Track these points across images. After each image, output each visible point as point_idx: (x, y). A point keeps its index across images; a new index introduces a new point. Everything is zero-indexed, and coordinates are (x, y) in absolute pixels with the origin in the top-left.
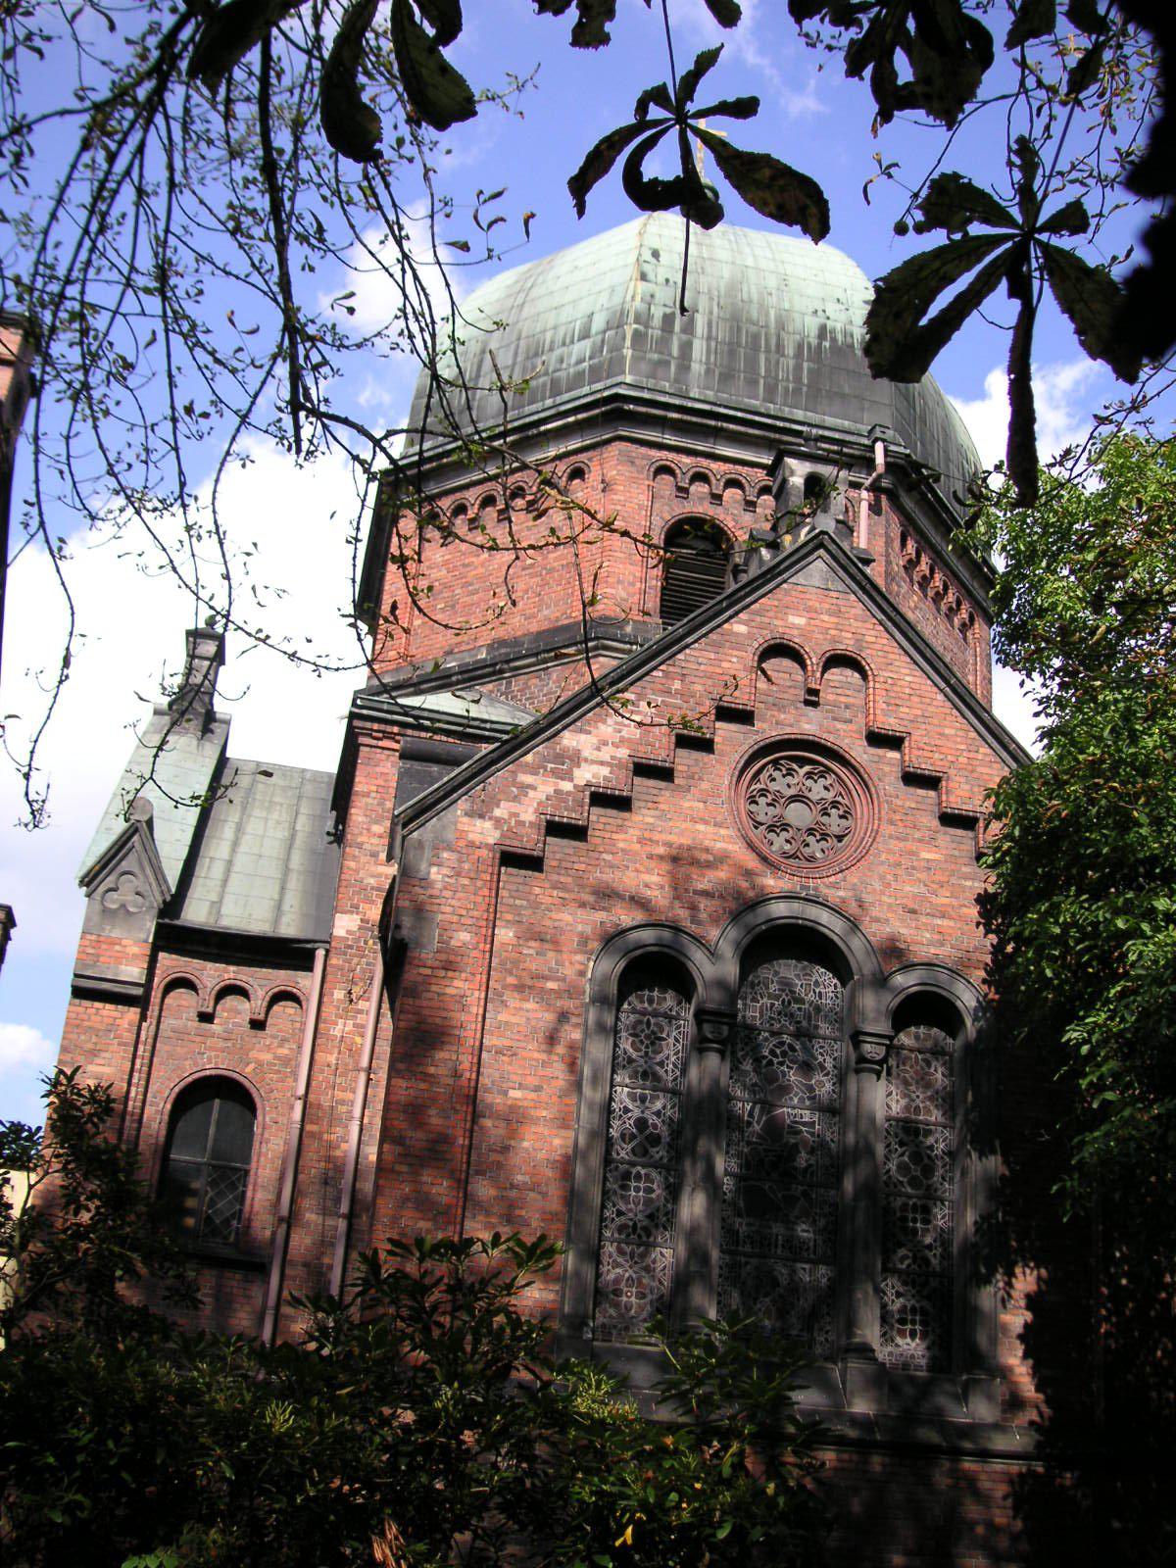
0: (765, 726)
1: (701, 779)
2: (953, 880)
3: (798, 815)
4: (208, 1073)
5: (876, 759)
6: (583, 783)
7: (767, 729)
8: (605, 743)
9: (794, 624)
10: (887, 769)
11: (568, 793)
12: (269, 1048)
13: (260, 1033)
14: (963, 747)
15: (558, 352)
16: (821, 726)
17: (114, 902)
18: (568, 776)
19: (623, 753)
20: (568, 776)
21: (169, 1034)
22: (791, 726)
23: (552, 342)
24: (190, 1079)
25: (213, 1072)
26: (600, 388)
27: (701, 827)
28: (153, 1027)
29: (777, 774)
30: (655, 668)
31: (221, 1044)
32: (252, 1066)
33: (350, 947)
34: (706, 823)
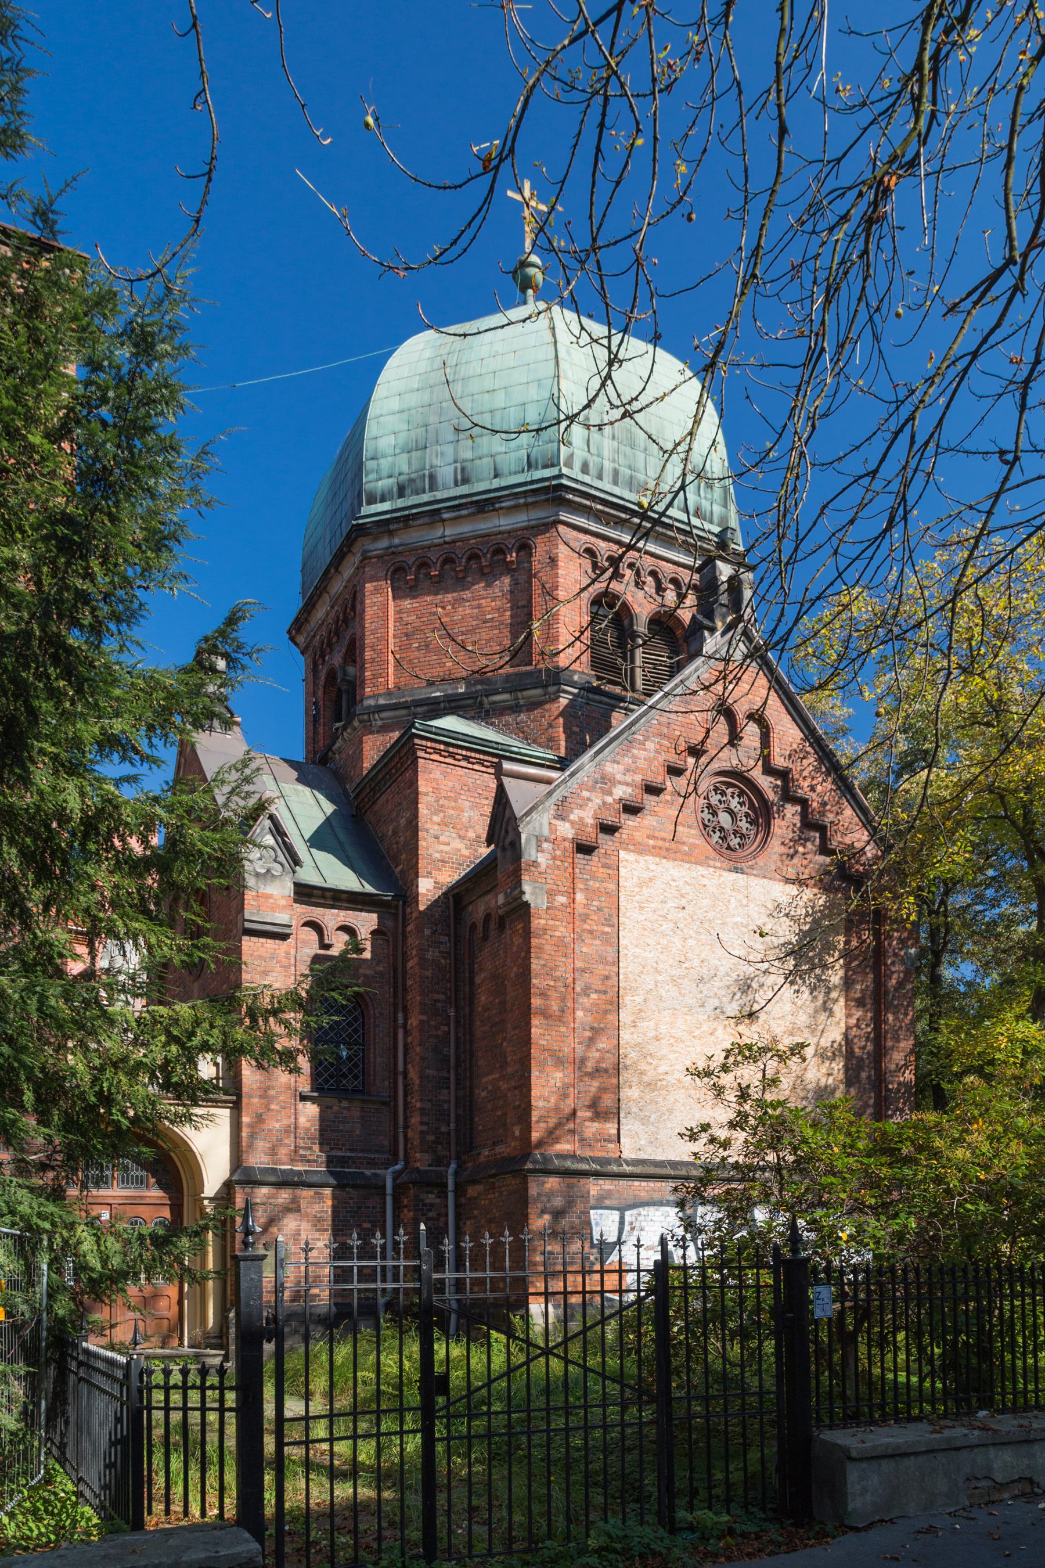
18: (610, 794)
19: (638, 778)
20: (610, 794)
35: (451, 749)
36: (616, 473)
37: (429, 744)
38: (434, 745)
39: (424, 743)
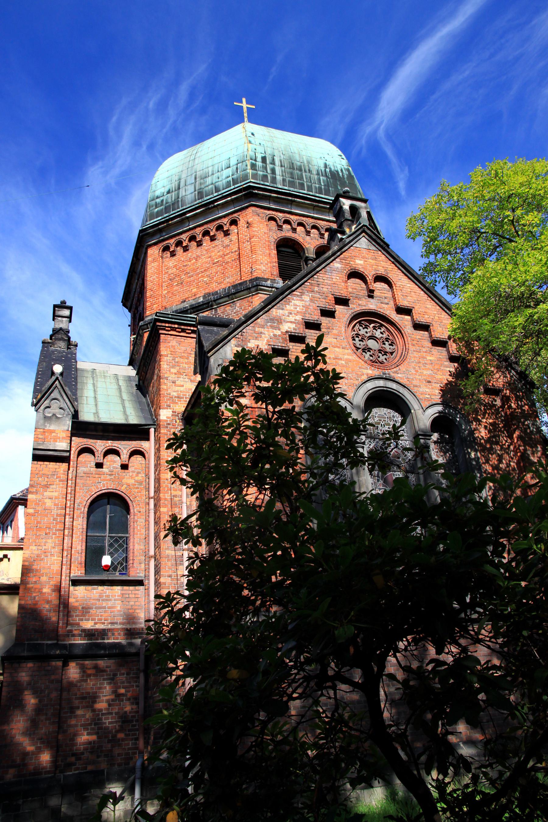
0: (355, 306)
1: (333, 329)
2: (442, 368)
3: (371, 344)
4: (104, 491)
5: (401, 319)
6: (284, 331)
7: (356, 307)
8: (291, 314)
9: (359, 264)
10: (406, 323)
11: (279, 335)
12: (132, 477)
13: (126, 471)
14: (435, 312)
15: (216, 175)
16: (376, 305)
17: (49, 413)
19: (299, 318)
21: (82, 474)
22: (365, 306)
24: (95, 495)
25: (106, 491)
26: (241, 185)
27: (337, 349)
28: (75, 472)
29: (361, 328)
30: (306, 282)
31: (108, 477)
32: (125, 486)
33: (169, 424)
34: (339, 347)
35: (183, 327)
36: (284, 180)
37: (167, 325)
38: (170, 325)
39: (163, 324)
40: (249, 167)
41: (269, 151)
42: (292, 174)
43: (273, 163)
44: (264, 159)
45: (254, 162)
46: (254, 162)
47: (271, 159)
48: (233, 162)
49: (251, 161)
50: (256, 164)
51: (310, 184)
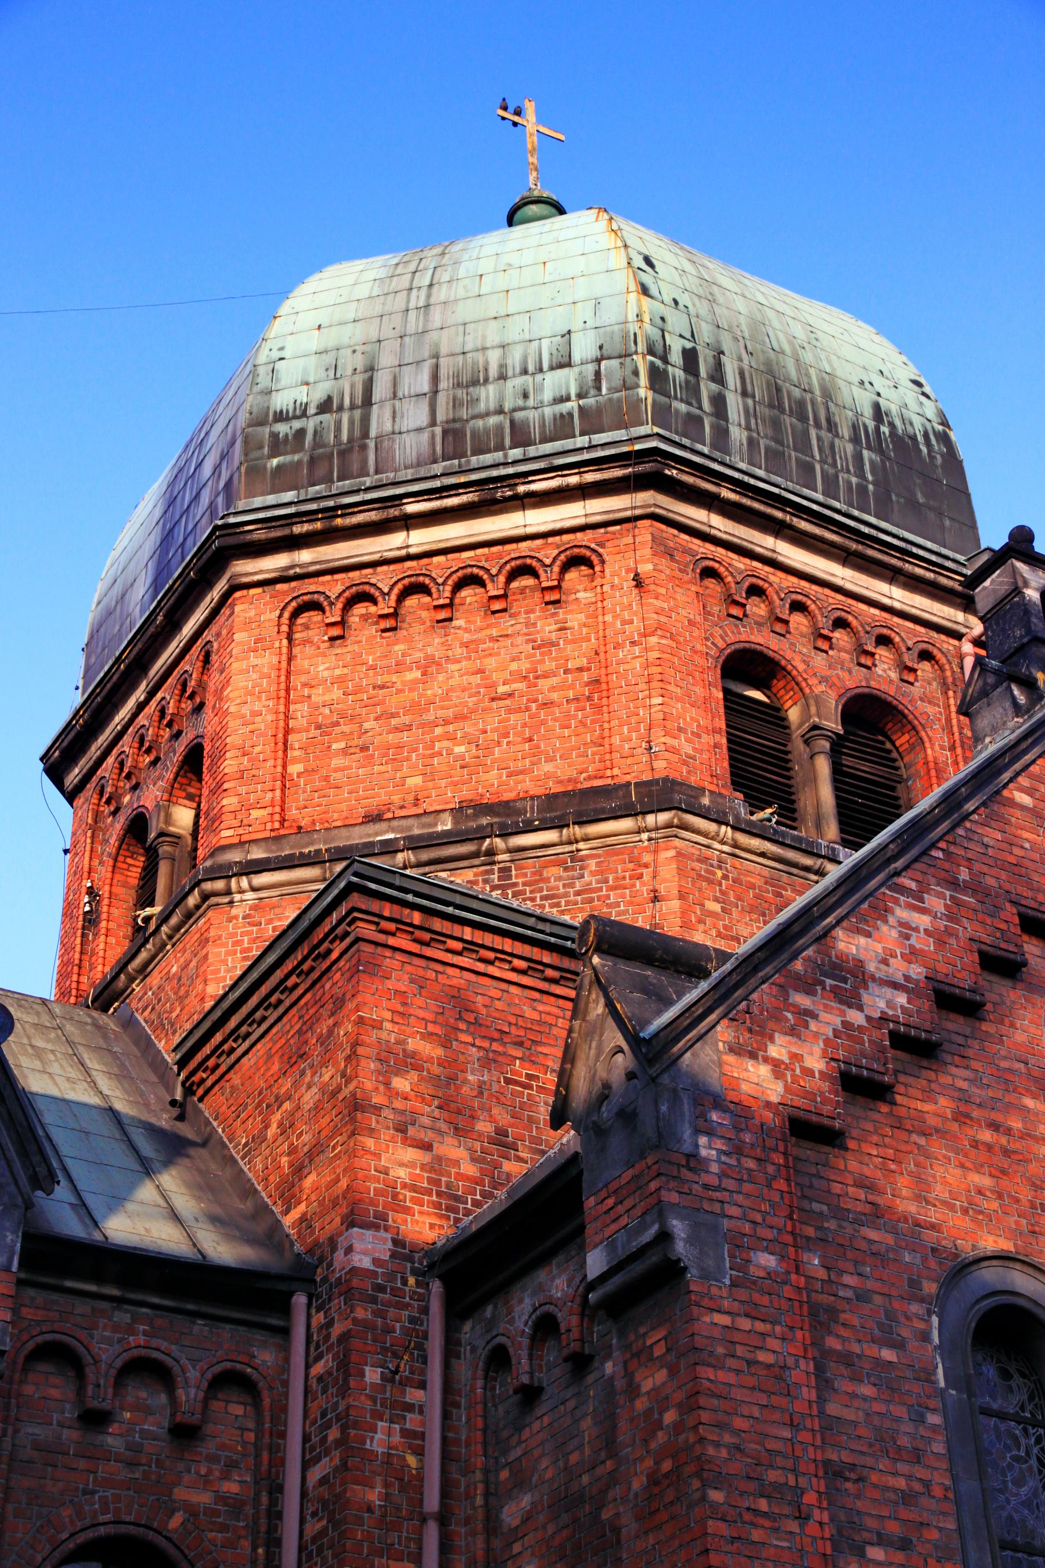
23: (503, 366)
36: (752, 443)
40: (643, 380)
41: (705, 333)
42: (776, 424)
43: (718, 376)
44: (690, 357)
45: (658, 363)
46: (658, 363)
47: (711, 360)
48: (584, 348)
49: (649, 358)
50: (666, 371)
51: (831, 471)
